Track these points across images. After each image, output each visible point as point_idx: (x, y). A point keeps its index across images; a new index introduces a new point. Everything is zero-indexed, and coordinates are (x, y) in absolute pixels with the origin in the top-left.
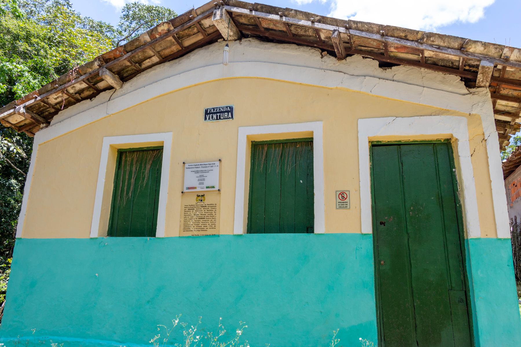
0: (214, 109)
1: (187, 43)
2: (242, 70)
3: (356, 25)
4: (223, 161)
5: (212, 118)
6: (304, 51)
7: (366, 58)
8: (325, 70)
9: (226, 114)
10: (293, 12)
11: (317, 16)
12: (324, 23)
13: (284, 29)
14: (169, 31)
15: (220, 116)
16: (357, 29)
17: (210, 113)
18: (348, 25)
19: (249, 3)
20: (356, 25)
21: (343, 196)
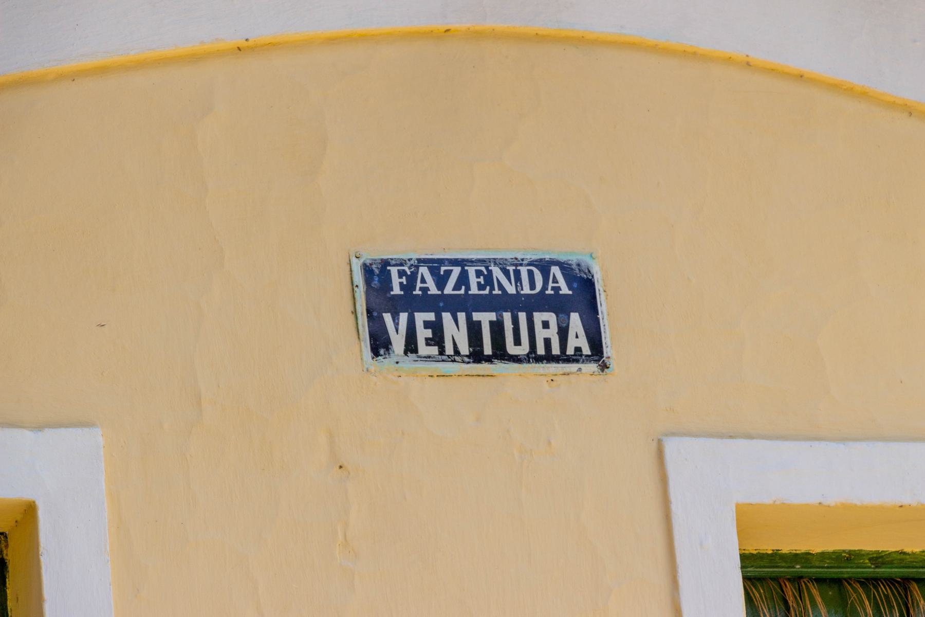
0: (434, 265)
5: (437, 339)
15: (497, 328)
17: (411, 301)
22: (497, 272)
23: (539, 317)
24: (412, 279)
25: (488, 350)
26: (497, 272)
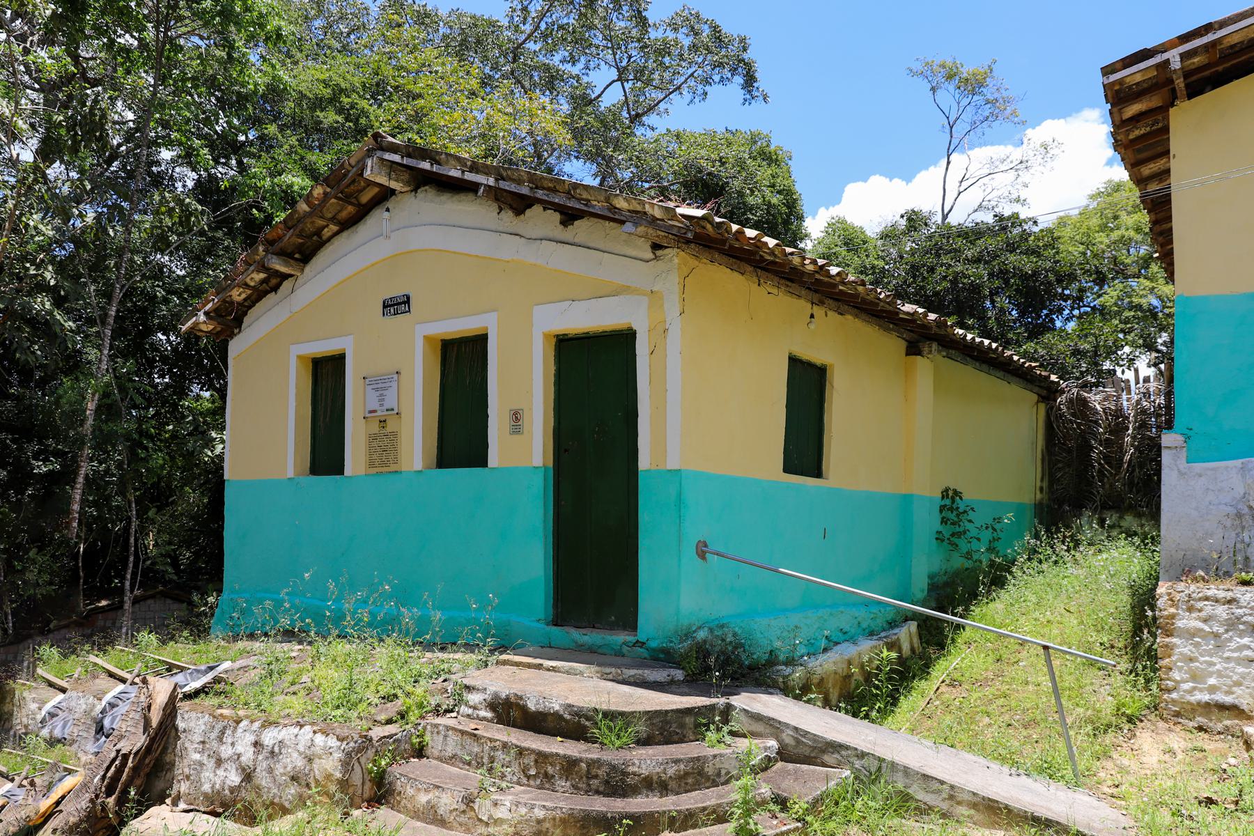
21: (516, 416)
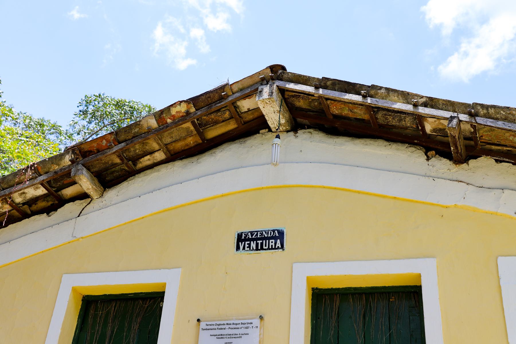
0: (252, 233)
1: (212, 133)
2: (298, 174)
3: (485, 111)
4: (266, 318)
5: (249, 247)
6: (398, 149)
7: (501, 162)
8: (434, 178)
9: (272, 242)
10: (383, 91)
11: (422, 97)
12: (432, 107)
13: (366, 117)
14: (188, 113)
15: (262, 244)
16: (487, 116)
17: (245, 240)
18: (473, 110)
19: (314, 78)
20: (485, 111)
22: (264, 233)
23: (271, 241)
24: (246, 235)
25: (259, 248)
26: (264, 233)
